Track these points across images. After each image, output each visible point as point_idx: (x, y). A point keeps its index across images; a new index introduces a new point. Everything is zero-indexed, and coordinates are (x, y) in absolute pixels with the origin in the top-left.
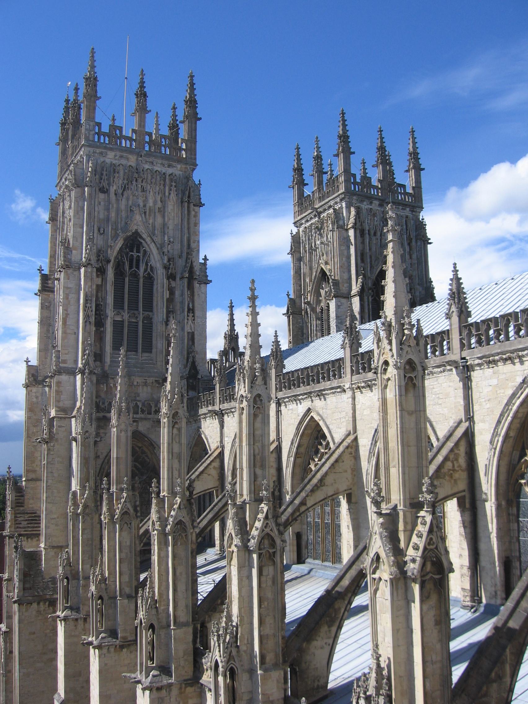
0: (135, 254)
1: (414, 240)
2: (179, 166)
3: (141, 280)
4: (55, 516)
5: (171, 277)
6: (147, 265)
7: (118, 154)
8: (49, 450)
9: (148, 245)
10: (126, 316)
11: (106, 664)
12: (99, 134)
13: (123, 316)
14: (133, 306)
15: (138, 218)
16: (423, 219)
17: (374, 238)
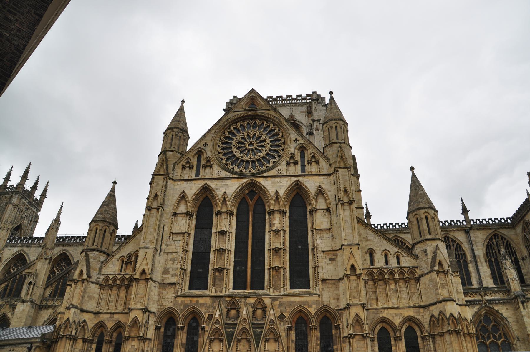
1: (33, 221)
17: (20, 213)
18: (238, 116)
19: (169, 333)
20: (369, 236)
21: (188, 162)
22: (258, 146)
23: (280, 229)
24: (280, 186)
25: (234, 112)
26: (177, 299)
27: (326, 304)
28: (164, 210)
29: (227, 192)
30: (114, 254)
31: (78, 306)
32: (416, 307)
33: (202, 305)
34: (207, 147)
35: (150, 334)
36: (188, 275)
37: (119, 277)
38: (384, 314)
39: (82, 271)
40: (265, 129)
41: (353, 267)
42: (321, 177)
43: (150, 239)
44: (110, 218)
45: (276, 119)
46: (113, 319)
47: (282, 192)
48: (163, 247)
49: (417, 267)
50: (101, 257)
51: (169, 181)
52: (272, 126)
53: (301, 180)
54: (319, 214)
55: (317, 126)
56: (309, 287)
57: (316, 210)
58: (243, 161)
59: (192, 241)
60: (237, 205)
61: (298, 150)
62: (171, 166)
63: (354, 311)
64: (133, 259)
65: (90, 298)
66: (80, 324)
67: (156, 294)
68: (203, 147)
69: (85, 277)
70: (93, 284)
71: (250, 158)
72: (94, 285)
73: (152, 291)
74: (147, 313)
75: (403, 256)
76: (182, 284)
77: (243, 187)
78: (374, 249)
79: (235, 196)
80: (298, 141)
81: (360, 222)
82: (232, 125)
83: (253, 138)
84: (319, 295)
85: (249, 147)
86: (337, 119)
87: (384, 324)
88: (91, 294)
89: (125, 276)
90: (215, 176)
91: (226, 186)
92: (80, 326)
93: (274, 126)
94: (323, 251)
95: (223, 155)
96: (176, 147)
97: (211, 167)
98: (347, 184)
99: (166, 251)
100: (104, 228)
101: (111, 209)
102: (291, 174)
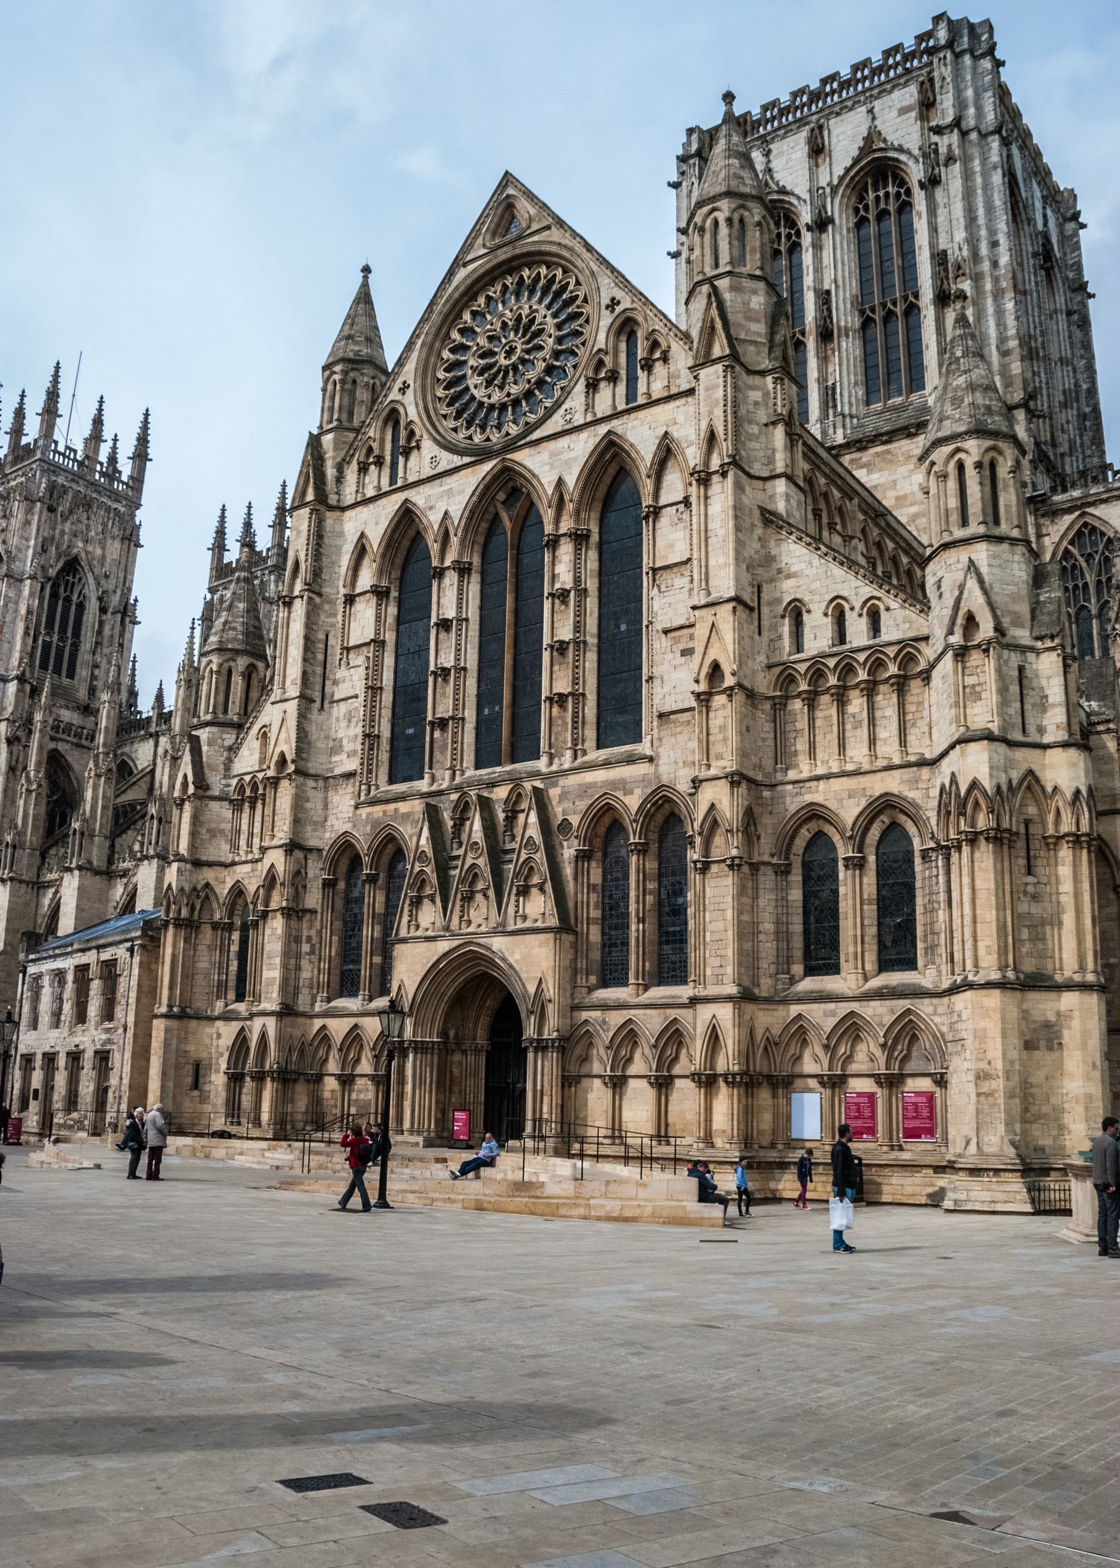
0: (70, 578)
3: (73, 607)
5: (103, 610)
10: (56, 637)
12: (55, 451)
18: (475, 276)
19: (356, 894)
20: (794, 560)
21: (370, 450)
22: (528, 352)
23: (568, 587)
24: (568, 463)
25: (465, 265)
26: (359, 812)
27: (665, 780)
28: (320, 595)
29: (450, 509)
32: (909, 765)
33: (406, 816)
34: (410, 393)
35: (313, 898)
36: (385, 745)
37: (260, 775)
38: (819, 794)
39: (185, 776)
40: (545, 291)
41: (716, 669)
42: (673, 405)
44: (235, 639)
45: (565, 253)
47: (571, 481)
48: (328, 690)
49: (926, 639)
51: (328, 514)
52: (559, 272)
53: (619, 431)
54: (664, 521)
55: (950, 146)
56: (638, 739)
57: (656, 512)
58: (492, 407)
59: (389, 660)
60: (481, 539)
61: (619, 333)
62: (330, 472)
63: (708, 795)
65: (213, 833)
67: (320, 806)
68: (399, 397)
69: (191, 790)
71: (509, 395)
73: (308, 800)
74: (298, 854)
75: (888, 609)
76: (370, 771)
77: (487, 487)
78: (806, 599)
79: (470, 518)
80: (619, 303)
81: (772, 522)
82: (466, 305)
83: (516, 332)
84: (651, 759)
85: (507, 362)
86: (714, 197)
87: (821, 822)
88: (213, 825)
90: (427, 472)
91: (450, 493)
92: (198, 897)
93: (565, 271)
94: (666, 632)
95: (449, 405)
96: (344, 416)
97: (418, 447)
98: (719, 412)
99: (336, 698)
100: (226, 665)
102: (599, 415)
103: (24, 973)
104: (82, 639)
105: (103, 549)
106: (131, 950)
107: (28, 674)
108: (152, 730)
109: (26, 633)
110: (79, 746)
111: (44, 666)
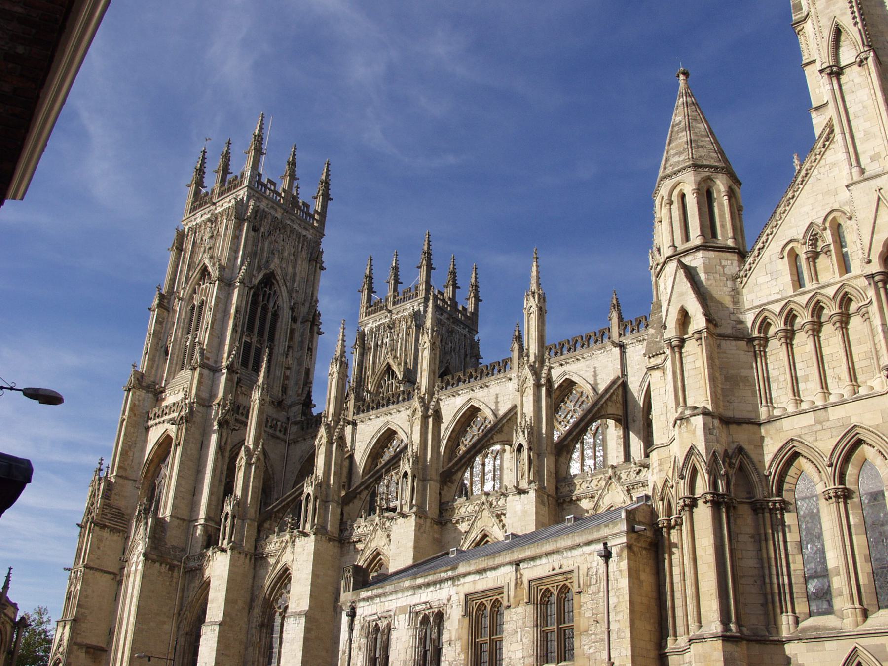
2: (311, 231)
3: (270, 315)
4: (183, 490)
5: (294, 319)
6: (275, 303)
7: (271, 204)
8: (187, 429)
9: (279, 287)
10: (255, 339)
11: (318, 549)
13: (251, 339)
14: (261, 334)
15: (276, 260)
16: (478, 340)
30: (760, 245)
31: (710, 407)
37: (803, 299)
43: (872, 153)
46: (827, 425)
50: (724, 263)
64: (828, 236)
66: (730, 459)
69: (698, 321)
70: (728, 342)
72: (734, 343)
88: (733, 372)
89: (822, 291)
101: (702, 136)
103: (352, 615)
104: (276, 342)
105: (294, 267)
106: (607, 555)
107: (235, 365)
108: (350, 418)
109: (234, 329)
110: (274, 436)
111: (245, 363)
